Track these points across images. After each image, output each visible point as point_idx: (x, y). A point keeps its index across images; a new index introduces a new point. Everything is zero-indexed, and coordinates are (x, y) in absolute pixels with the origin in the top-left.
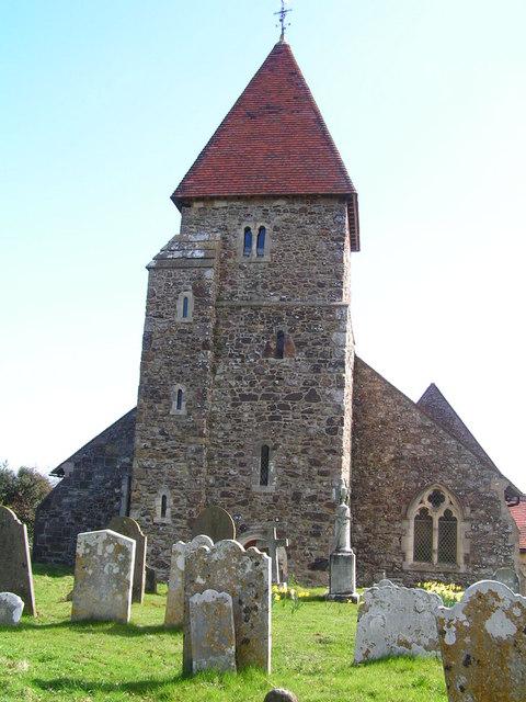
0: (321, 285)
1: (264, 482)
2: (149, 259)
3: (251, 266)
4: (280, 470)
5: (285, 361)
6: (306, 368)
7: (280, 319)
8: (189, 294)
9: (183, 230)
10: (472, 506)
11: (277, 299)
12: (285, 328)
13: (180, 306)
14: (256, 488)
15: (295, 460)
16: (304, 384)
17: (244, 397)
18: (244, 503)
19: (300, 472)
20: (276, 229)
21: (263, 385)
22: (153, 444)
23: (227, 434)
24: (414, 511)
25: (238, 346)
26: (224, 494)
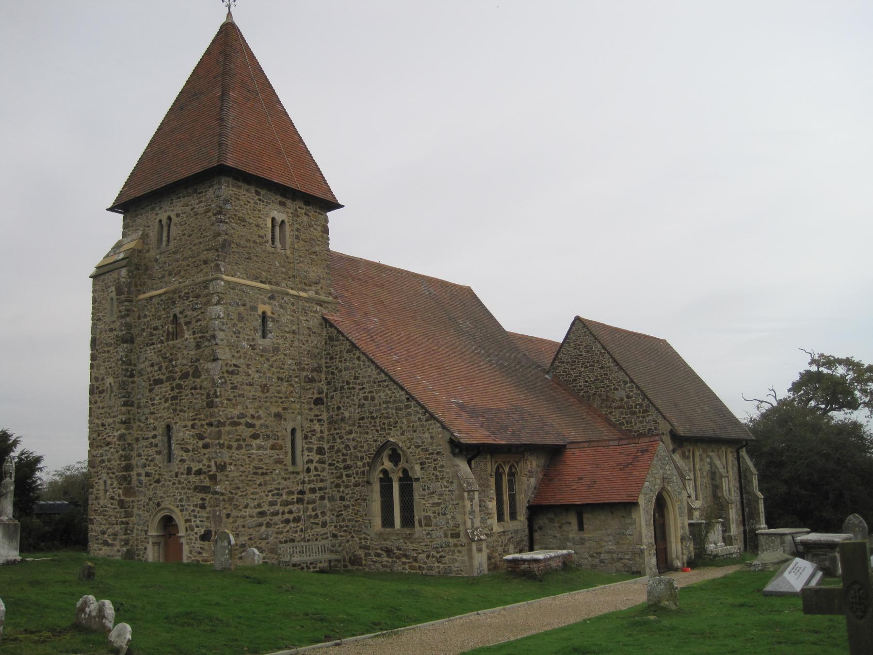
2: (92, 270)
9: (124, 235)
10: (421, 464)
17: (158, 382)
18: (158, 481)
19: (190, 448)
22: (99, 435)
23: (147, 419)
24: (377, 475)
25: (152, 335)
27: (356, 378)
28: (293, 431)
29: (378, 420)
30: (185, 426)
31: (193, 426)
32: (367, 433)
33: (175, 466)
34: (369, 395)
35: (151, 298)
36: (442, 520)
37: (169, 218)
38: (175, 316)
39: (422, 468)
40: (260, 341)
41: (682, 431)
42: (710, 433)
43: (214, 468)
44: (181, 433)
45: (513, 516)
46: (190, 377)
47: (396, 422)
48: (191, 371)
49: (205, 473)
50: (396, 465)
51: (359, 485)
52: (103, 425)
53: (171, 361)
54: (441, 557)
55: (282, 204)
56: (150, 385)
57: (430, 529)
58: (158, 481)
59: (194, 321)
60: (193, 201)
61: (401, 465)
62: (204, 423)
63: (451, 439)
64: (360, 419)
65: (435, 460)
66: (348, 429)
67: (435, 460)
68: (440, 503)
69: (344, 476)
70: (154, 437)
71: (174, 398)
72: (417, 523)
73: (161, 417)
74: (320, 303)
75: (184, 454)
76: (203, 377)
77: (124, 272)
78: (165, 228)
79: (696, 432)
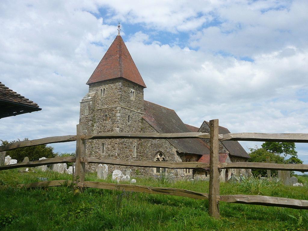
0: (115, 102)
1: (103, 153)
3: (102, 99)
4: (106, 149)
5: (107, 122)
6: (111, 123)
7: (106, 112)
8: (87, 108)
10: (168, 157)
11: (106, 106)
13: (86, 111)
14: (102, 154)
15: (109, 146)
20: (107, 89)
28: (134, 146)
37: (104, 89)
38: (106, 115)
40: (128, 123)
41: (232, 154)
42: (239, 155)
43: (117, 155)
45: (189, 172)
49: (114, 156)
50: (161, 157)
53: (104, 127)
55: (134, 87)
60: (112, 85)
61: (163, 157)
63: (177, 151)
70: (99, 146)
74: (142, 114)
77: (91, 102)
78: (103, 92)
79: (236, 154)
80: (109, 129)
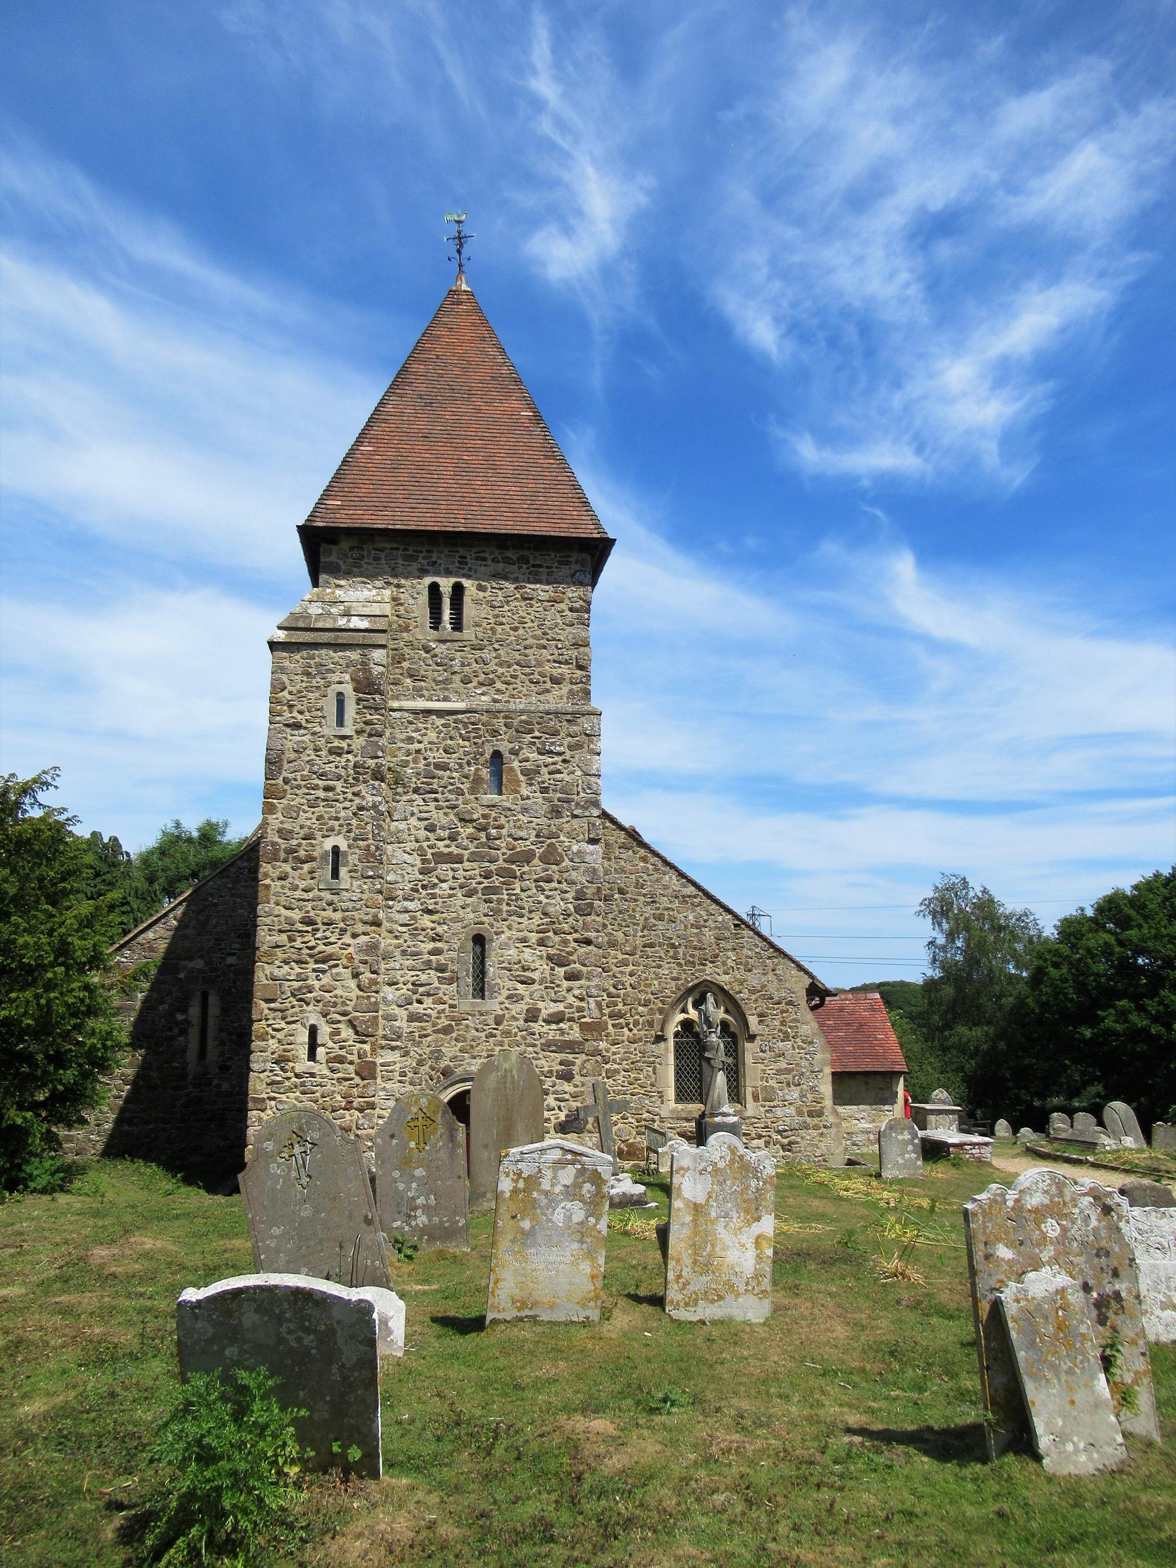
0: (556, 681)
12: (504, 747)
16: (537, 836)
19: (536, 976)
21: (472, 838)
22: (291, 939)
26: (413, 1018)
27: (639, 885)
29: (681, 950)
30: (524, 940)
31: (542, 943)
32: (659, 967)
33: (493, 1005)
34: (666, 913)
35: (428, 712)
36: (794, 1094)
38: (497, 755)
39: (760, 1022)
44: (504, 951)
46: (536, 861)
47: (716, 956)
48: (538, 852)
49: (571, 1020)
51: (640, 1040)
52: (310, 922)
54: (790, 1143)
56: (424, 861)
57: (772, 1104)
58: (447, 1030)
59: (544, 770)
62: (568, 937)
64: (644, 946)
65: (782, 1012)
66: (621, 957)
67: (782, 1012)
68: (793, 1070)
69: (610, 1027)
70: (436, 952)
71: (488, 890)
72: (749, 1097)
73: (454, 920)
75: (519, 986)
76: (566, 863)
80: (521, 846)
